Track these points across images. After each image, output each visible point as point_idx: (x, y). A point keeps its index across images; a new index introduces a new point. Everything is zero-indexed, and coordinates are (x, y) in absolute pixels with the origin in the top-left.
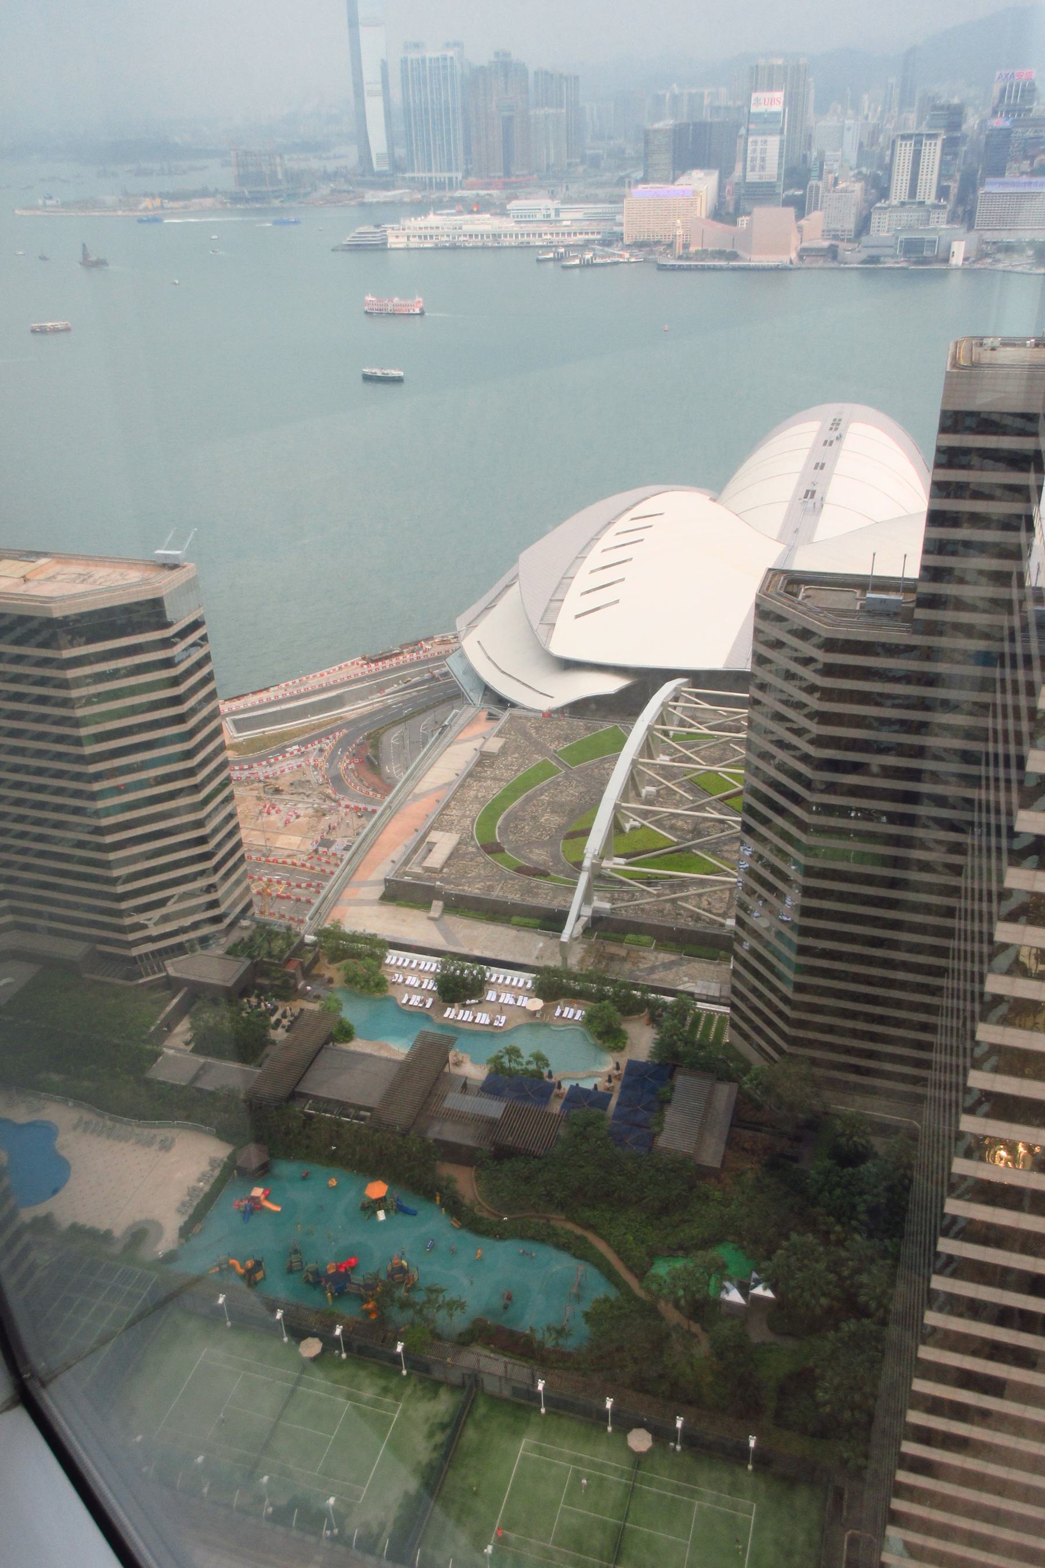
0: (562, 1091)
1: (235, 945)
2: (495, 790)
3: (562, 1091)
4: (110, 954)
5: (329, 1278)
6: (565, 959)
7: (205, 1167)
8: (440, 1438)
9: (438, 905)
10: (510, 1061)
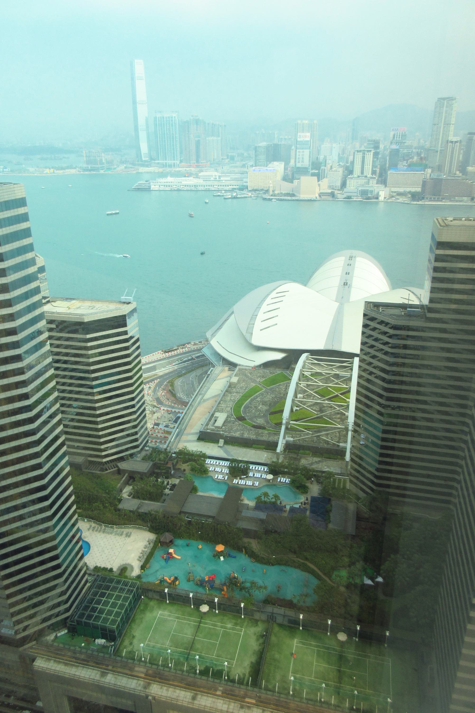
0: (286, 509)
1: (145, 456)
2: (238, 397)
3: (286, 509)
4: (93, 461)
5: (206, 582)
6: (278, 459)
7: (146, 543)
8: (261, 641)
9: (222, 441)
10: (264, 498)
